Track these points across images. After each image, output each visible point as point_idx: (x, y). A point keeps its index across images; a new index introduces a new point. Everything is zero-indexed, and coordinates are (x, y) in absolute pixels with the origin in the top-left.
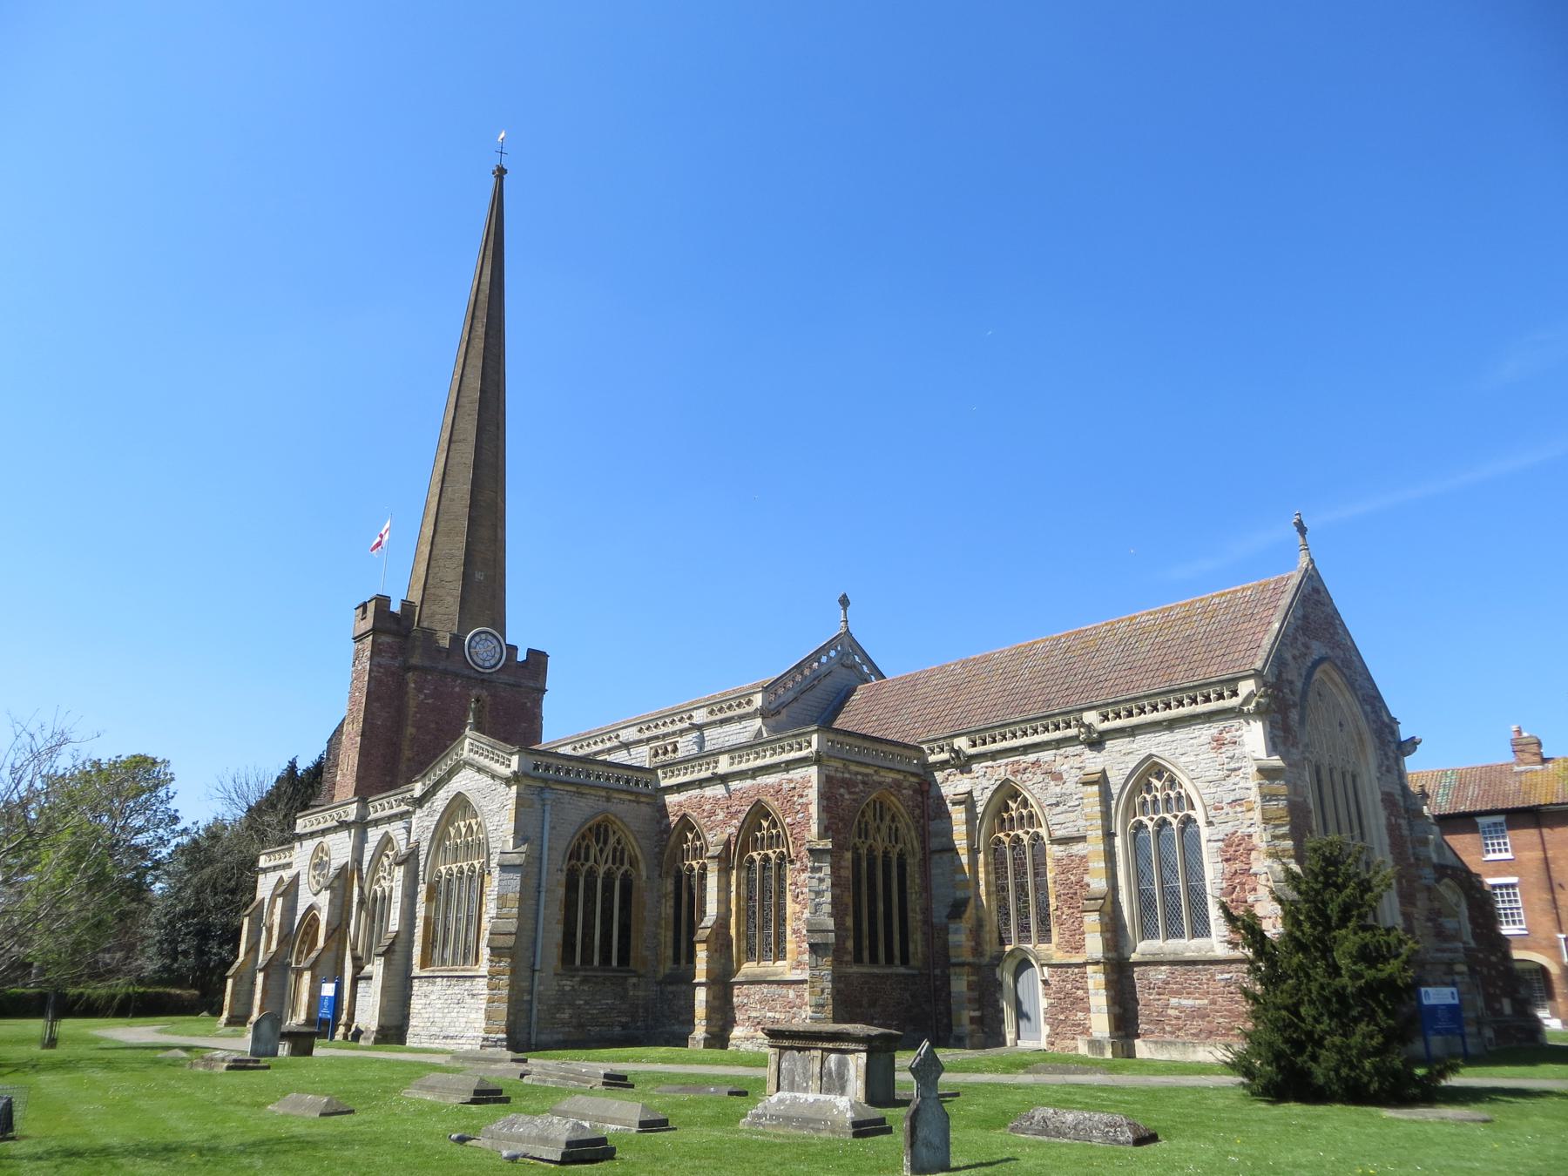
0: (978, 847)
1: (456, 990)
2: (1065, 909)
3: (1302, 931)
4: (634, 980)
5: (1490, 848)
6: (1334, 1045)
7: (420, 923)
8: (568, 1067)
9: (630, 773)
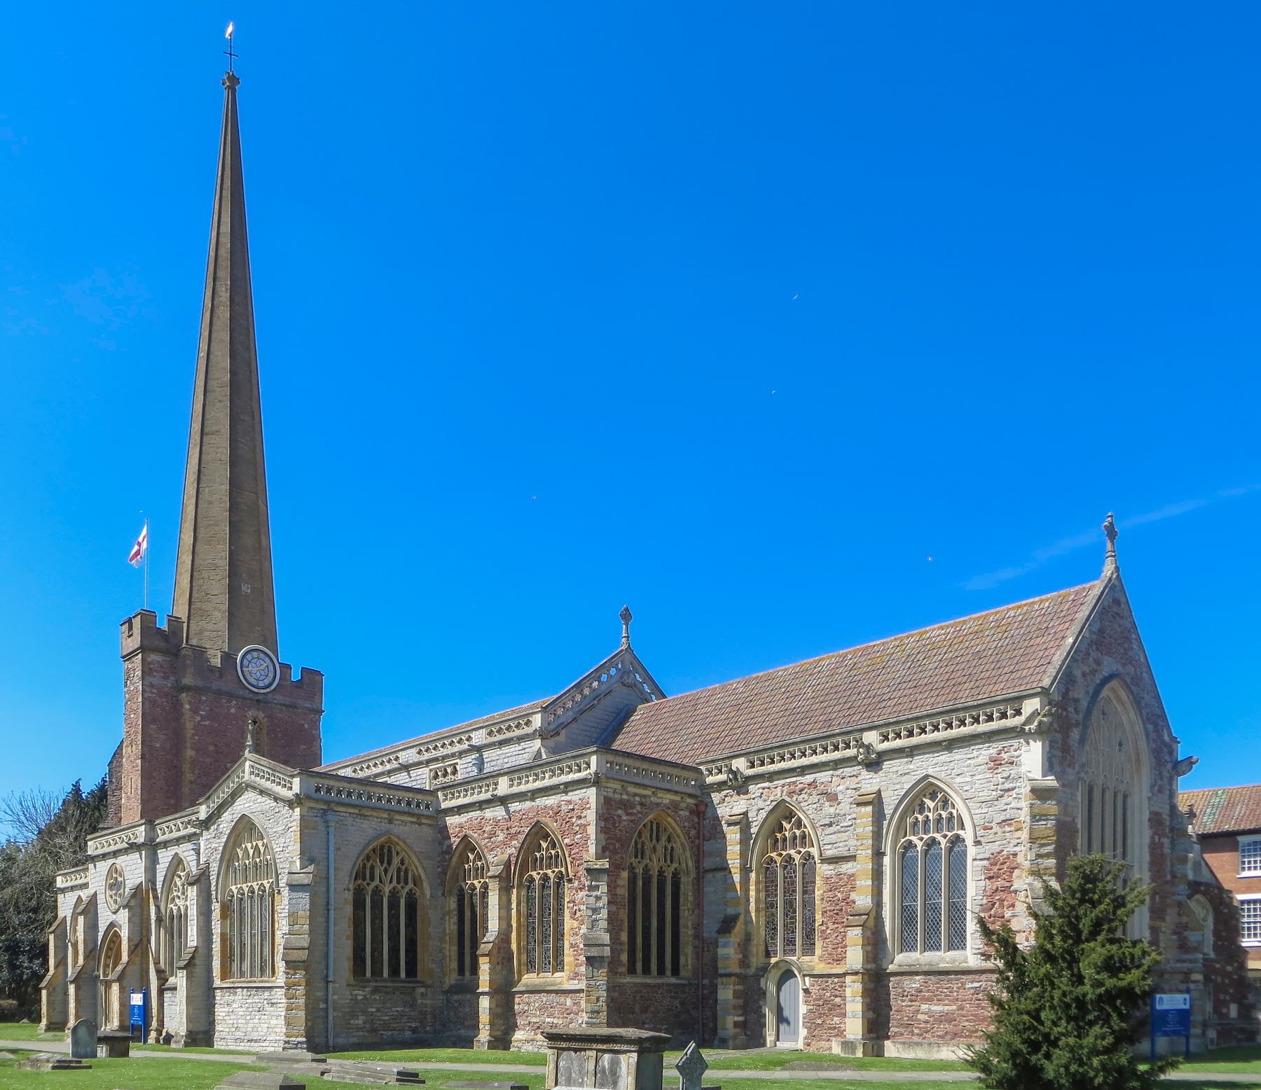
0: (751, 867)
1: (256, 999)
2: (830, 924)
3: (1053, 944)
4: (422, 990)
5: (1246, 866)
6: (1067, 1045)
7: (217, 939)
8: (365, 1066)
9: (411, 795)
